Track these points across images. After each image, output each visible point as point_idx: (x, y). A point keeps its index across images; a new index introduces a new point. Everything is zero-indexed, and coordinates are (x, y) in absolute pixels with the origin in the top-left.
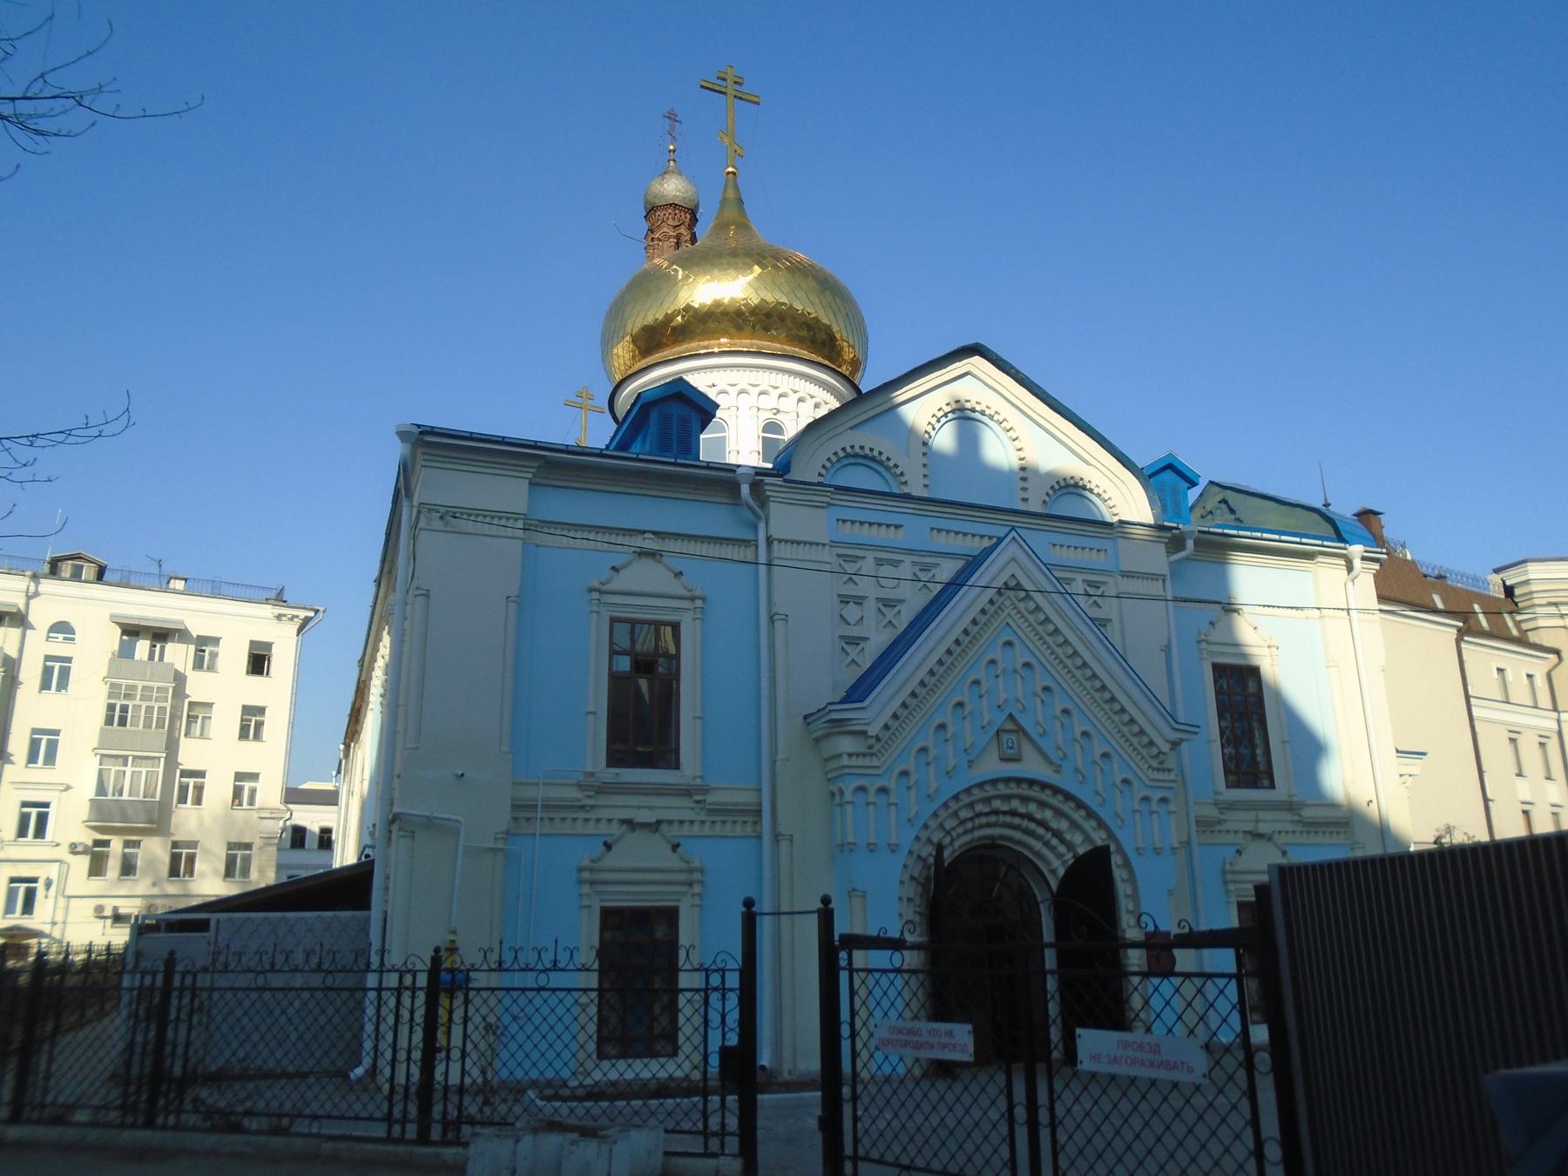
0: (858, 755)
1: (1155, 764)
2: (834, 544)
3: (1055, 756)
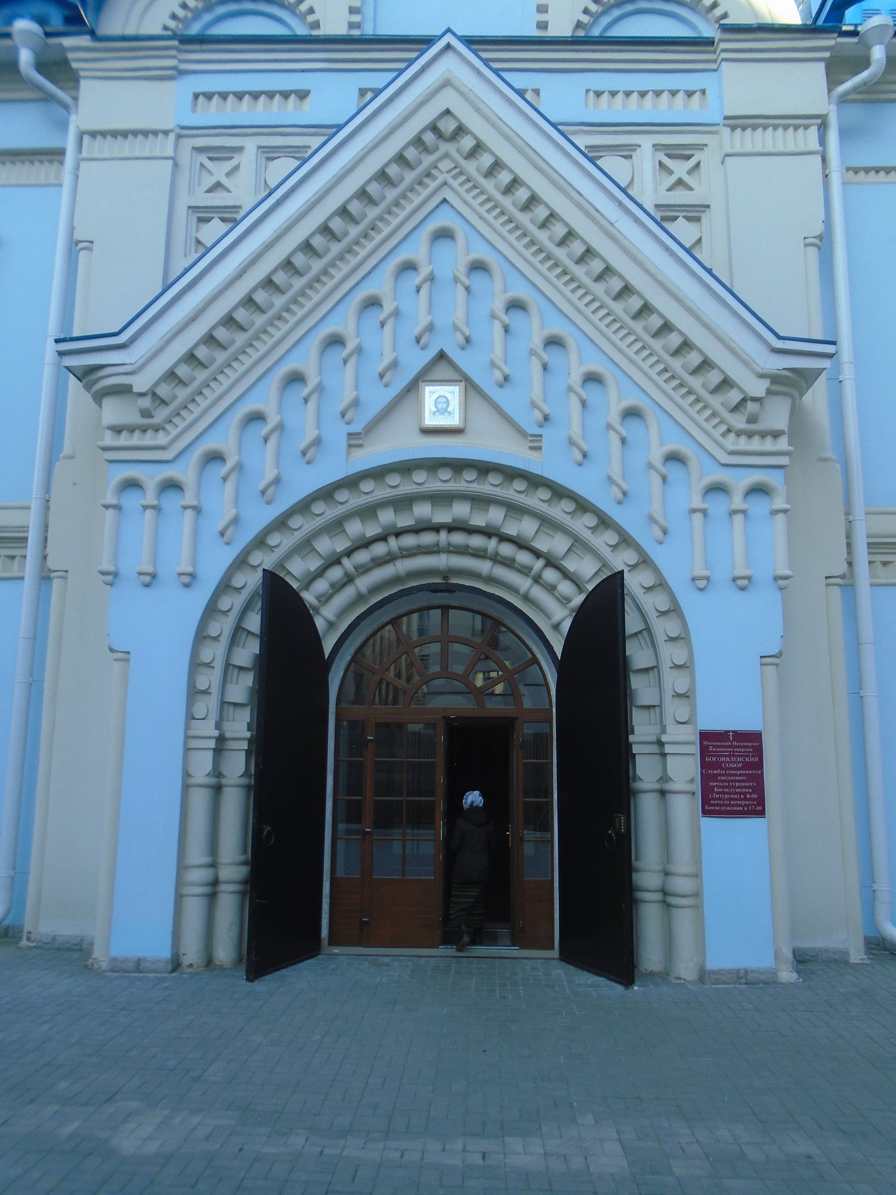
0: (132, 430)
1: (738, 422)
2: (184, 132)
3: (529, 421)
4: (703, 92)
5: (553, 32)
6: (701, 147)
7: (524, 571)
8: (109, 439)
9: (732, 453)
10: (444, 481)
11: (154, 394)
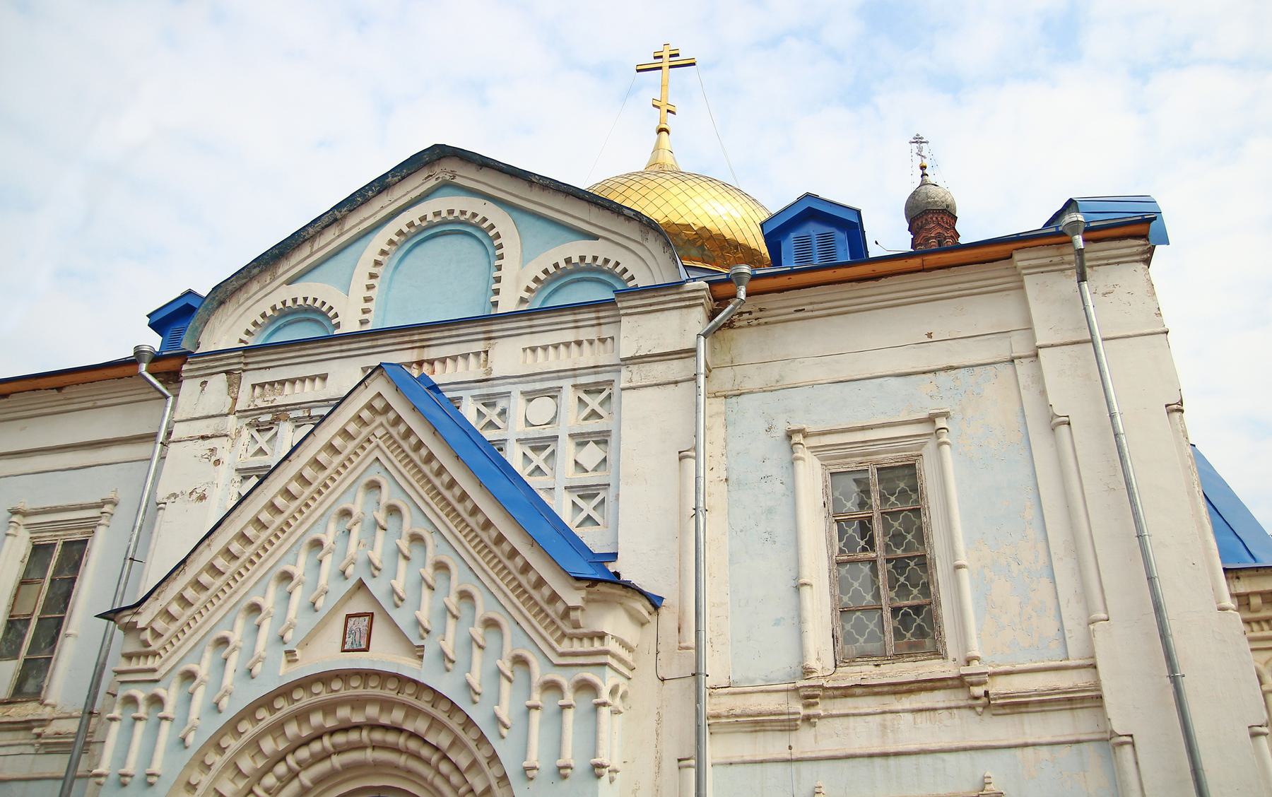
4: (612, 338)
5: (501, 310)
6: (610, 382)
7: (427, 762)
8: (124, 665)
9: (563, 655)
10: (356, 689)
11: (153, 630)
